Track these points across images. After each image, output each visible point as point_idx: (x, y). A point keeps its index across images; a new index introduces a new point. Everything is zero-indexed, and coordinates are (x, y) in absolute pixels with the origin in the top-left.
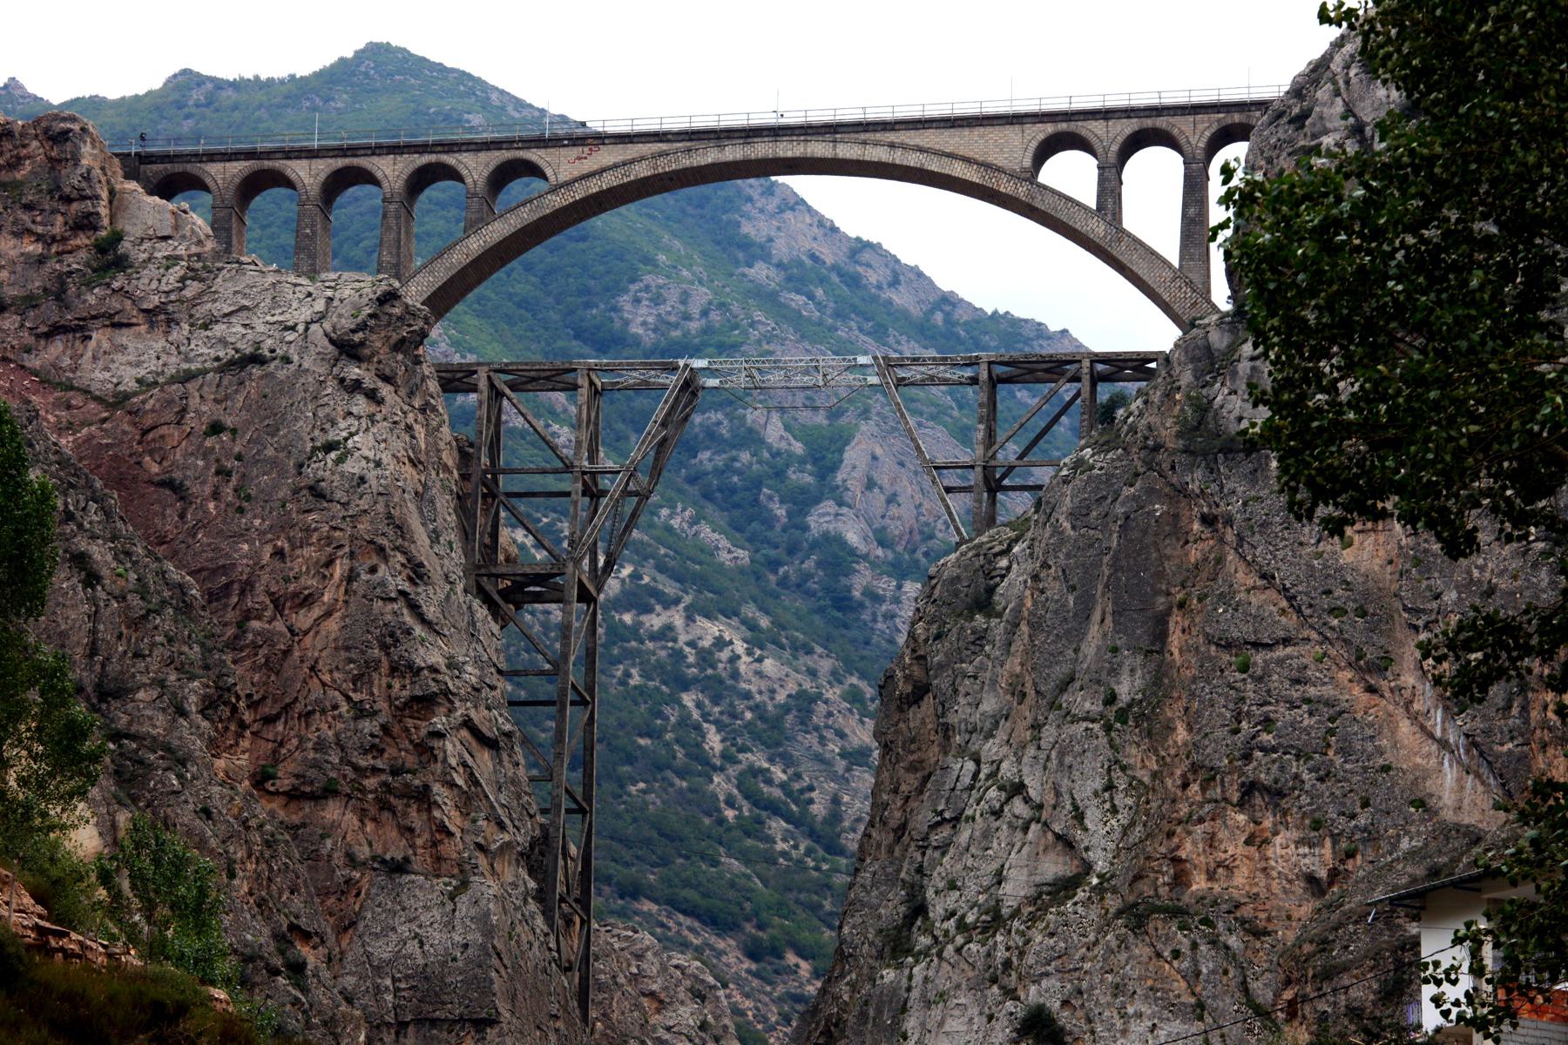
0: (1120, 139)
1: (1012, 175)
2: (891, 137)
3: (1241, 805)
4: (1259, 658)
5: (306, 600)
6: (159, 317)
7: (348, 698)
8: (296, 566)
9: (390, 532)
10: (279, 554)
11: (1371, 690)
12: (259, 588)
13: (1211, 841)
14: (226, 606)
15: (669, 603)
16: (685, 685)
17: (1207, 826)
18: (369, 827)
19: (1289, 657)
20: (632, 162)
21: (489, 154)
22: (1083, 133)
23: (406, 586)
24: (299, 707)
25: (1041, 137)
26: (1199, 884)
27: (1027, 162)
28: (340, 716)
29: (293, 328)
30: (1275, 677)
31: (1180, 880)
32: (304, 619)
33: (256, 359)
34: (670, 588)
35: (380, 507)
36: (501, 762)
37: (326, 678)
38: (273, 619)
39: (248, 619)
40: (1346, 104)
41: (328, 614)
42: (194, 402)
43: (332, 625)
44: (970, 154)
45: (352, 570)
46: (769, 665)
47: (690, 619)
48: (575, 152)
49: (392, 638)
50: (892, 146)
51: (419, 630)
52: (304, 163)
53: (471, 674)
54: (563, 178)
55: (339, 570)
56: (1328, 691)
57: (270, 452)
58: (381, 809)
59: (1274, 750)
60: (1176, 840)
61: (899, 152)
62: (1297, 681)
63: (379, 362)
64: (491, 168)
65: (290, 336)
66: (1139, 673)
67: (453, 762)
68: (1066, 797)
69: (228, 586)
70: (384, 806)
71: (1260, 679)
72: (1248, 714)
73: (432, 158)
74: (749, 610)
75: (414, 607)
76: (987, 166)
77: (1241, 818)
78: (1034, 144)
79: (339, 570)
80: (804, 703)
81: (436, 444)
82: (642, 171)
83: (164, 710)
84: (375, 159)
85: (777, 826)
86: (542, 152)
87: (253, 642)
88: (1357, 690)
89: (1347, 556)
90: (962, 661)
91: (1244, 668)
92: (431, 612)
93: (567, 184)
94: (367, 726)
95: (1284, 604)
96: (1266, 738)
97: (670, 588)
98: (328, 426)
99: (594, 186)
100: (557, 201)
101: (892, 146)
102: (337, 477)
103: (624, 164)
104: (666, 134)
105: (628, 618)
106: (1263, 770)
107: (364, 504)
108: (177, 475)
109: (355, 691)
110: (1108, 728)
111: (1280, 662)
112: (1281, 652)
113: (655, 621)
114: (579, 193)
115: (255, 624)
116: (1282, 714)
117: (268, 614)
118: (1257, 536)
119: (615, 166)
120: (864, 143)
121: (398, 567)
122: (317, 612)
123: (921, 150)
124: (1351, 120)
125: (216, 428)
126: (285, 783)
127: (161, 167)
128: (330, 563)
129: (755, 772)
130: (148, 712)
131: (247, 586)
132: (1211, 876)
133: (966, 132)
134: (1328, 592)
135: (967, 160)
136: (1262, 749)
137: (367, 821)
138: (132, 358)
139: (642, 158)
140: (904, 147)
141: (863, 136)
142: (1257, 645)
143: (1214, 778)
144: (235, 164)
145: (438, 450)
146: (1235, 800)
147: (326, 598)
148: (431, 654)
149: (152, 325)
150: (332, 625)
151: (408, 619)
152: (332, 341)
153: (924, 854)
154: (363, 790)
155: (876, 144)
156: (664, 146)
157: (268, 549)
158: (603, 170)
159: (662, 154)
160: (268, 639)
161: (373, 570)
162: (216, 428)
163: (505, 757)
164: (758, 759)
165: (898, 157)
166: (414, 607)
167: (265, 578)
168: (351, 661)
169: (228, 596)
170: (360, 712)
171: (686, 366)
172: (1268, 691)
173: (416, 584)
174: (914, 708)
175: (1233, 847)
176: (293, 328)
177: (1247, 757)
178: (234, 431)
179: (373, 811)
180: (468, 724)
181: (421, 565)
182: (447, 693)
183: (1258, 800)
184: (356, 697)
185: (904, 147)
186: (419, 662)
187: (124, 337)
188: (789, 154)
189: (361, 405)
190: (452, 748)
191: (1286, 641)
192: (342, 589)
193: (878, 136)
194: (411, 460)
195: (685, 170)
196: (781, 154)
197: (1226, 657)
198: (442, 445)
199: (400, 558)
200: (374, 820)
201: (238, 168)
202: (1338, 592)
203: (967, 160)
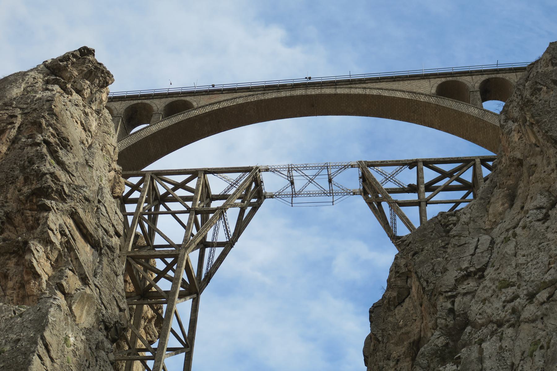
0: (480, 82)
20: (236, 98)
21: (167, 99)
25: (439, 82)
36: (100, 262)
61: (368, 90)
63: (74, 82)
73: (140, 101)
86: (192, 98)
90: (437, 257)
93: (203, 107)
101: (365, 88)
103: (231, 99)
120: (351, 88)
133: (401, 82)
135: (404, 91)
153: (453, 303)
163: (105, 260)
174: (399, 307)
188: (313, 93)
195: (261, 100)
203: (404, 91)
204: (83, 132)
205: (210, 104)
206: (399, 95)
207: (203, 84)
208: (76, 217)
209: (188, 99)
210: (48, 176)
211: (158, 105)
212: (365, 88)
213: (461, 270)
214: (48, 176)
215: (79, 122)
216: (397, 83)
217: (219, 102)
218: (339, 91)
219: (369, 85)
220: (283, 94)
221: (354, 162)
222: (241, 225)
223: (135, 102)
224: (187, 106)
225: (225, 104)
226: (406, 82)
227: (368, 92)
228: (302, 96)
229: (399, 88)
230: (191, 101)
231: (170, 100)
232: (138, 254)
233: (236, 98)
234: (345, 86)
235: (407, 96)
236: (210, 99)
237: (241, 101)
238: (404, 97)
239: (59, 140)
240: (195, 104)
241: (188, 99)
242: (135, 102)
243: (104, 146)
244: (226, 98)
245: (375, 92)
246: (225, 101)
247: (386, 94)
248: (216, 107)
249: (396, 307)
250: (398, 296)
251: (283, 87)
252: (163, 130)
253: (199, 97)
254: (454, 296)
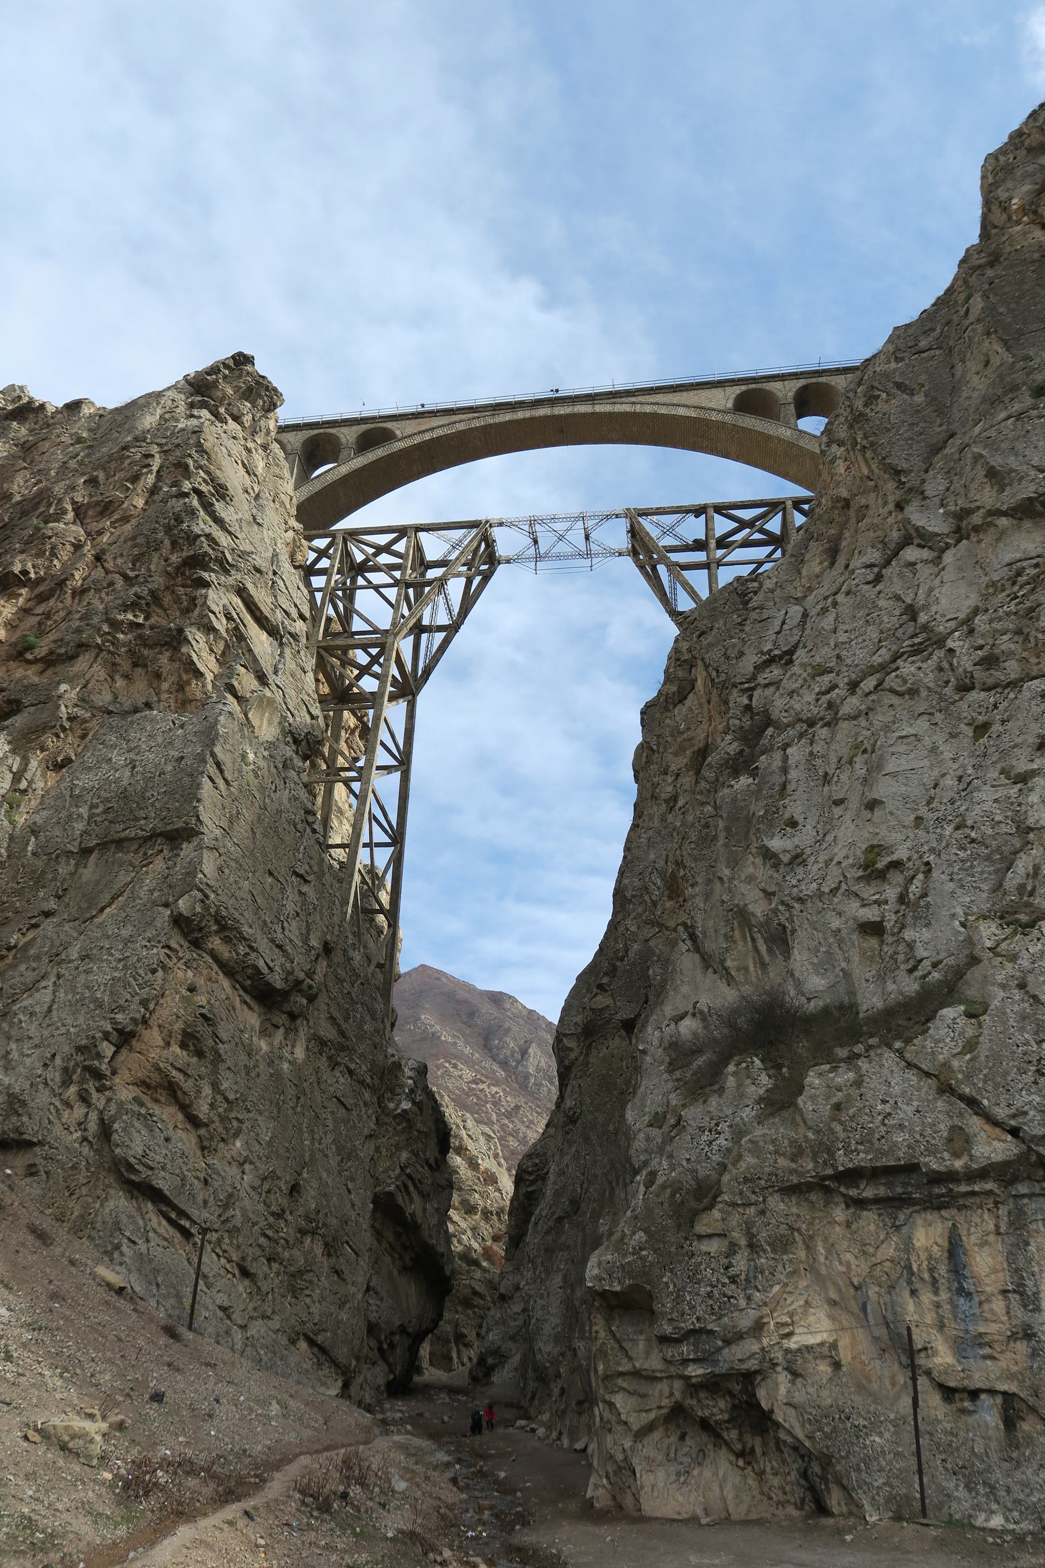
0: (795, 390)
15: (483, 1082)
16: (487, 1102)
18: (120, 683)
25: (738, 392)
34: (484, 1079)
36: (281, 655)
37: (110, 565)
46: (509, 1098)
47: (489, 1086)
58: (135, 665)
61: (639, 406)
63: (229, 404)
70: (138, 662)
73: (322, 431)
74: (504, 1087)
80: (517, 1107)
85: (510, 1138)
86: (394, 423)
90: (732, 638)
93: (410, 436)
97: (484, 1079)
101: (634, 403)
104: (477, 407)
105: (474, 1086)
109: (133, 570)
113: (481, 1086)
129: (504, 1125)
133: (685, 394)
135: (688, 406)
137: (117, 677)
153: (750, 698)
154: (115, 642)
159: (474, 418)
163: (287, 651)
164: (506, 1121)
174: (680, 706)
179: (125, 665)
188: (562, 412)
195: (490, 425)
200: (126, 677)
203: (688, 406)
204: (246, 476)
205: (420, 432)
206: (681, 411)
207: (408, 404)
208: (245, 595)
209: (389, 425)
210: (202, 539)
211: (348, 436)
212: (634, 403)
213: (762, 653)
214: (202, 539)
215: (239, 462)
216: (678, 394)
217: (432, 429)
218: (599, 408)
219: (640, 399)
220: (520, 415)
221: (619, 509)
222: (469, 601)
223: (316, 432)
224: (387, 436)
225: (440, 432)
226: (691, 393)
227: (638, 408)
228: (546, 417)
230: (393, 428)
231: (364, 427)
232: (331, 643)
234: (606, 401)
235: (692, 413)
236: (419, 424)
237: (461, 427)
238: (688, 414)
239: (214, 487)
240: (398, 433)
241: (389, 425)
242: (316, 432)
243: (277, 495)
244: (441, 423)
245: (648, 409)
246: (440, 428)
247: (663, 410)
248: (427, 436)
249: (675, 706)
250: (679, 692)
251: (520, 405)
252: (356, 471)
253: (404, 422)
254: (753, 689)
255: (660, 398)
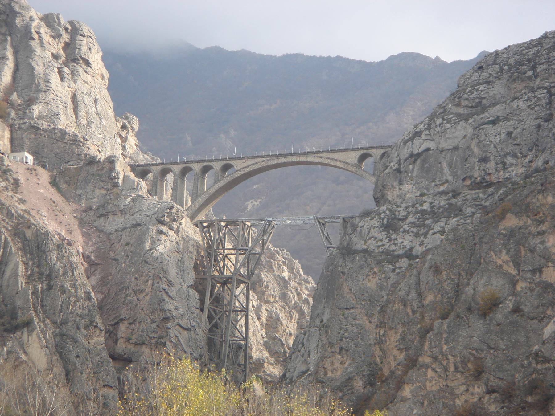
0: (380, 154)
1: (352, 165)
2: (321, 155)
3: (340, 353)
4: (347, 312)
5: (142, 291)
6: (123, 212)
7: (150, 318)
8: (140, 282)
9: (162, 273)
10: (136, 279)
11: (370, 322)
12: (130, 288)
13: (332, 363)
14: (122, 293)
17: (331, 359)
19: (353, 312)
20: (256, 163)
22: (371, 153)
23: (166, 287)
24: (138, 320)
25: (360, 154)
26: (330, 374)
27: (356, 161)
28: (148, 322)
29: (149, 216)
30: (350, 318)
31: (326, 374)
32: (141, 296)
33: (138, 225)
35: (161, 266)
37: (145, 312)
38: (134, 296)
39: (127, 296)
40: (398, 153)
41: (147, 295)
42: (124, 237)
43: (148, 298)
44: (341, 160)
45: (153, 283)
48: (242, 161)
49: (161, 301)
50: (321, 157)
51: (167, 299)
52: (176, 166)
53: (181, 311)
54: (239, 168)
55: (150, 283)
56: (360, 322)
57: (138, 251)
59: (347, 338)
60: (324, 362)
62: (354, 319)
64: (221, 166)
65: (148, 218)
66: (329, 314)
67: (172, 335)
68: (308, 348)
69: (123, 288)
71: (346, 318)
72: (343, 328)
75: (167, 293)
76: (345, 163)
77: (339, 357)
78: (358, 156)
79: (150, 283)
81: (187, 246)
82: (258, 166)
83: (73, 328)
84: (193, 164)
86: (234, 161)
87: (128, 303)
88: (367, 322)
89: (369, 285)
91: (343, 315)
92: (171, 294)
94: (154, 326)
95: (354, 297)
96: (346, 334)
98: (153, 243)
99: (246, 171)
100: (237, 175)
101: (321, 157)
102: (151, 258)
103: (254, 164)
106: (344, 344)
107: (157, 265)
108: (117, 257)
109: (152, 316)
110: (320, 330)
111: (351, 314)
112: (352, 311)
114: (242, 172)
115: (129, 298)
116: (350, 328)
117: (132, 295)
118: (350, 279)
119: (252, 165)
120: (314, 157)
121: (164, 282)
122: (144, 294)
123: (329, 158)
124: (398, 158)
125: (128, 244)
126: (133, 341)
127: (141, 168)
128: (147, 281)
130: (70, 329)
131: (128, 288)
132: (332, 372)
134: (363, 295)
135: (340, 161)
136: (345, 338)
138: (116, 223)
139: (259, 162)
140: (325, 158)
141: (314, 155)
142: (346, 309)
143: (333, 346)
144: (159, 166)
145: (188, 248)
146: (338, 352)
147: (146, 291)
148: (170, 306)
149: (122, 214)
150: (148, 298)
151: (165, 296)
152: (156, 220)
154: (151, 343)
155: (318, 157)
156: (264, 159)
157: (134, 278)
158: (249, 166)
160: (131, 302)
161: (158, 283)
162: (128, 244)
165: (322, 161)
166: (167, 293)
167: (132, 285)
168: (151, 308)
169: (123, 290)
170: (153, 322)
171: (266, 220)
172: (348, 322)
173: (169, 286)
175: (337, 365)
176: (149, 216)
177: (341, 340)
178: (132, 245)
180: (179, 325)
181: (170, 281)
182: (172, 317)
183: (344, 352)
184: (152, 317)
185: (325, 158)
186: (166, 308)
187: (116, 218)
188: (296, 161)
189: (163, 237)
190: (172, 332)
191: (353, 308)
192: (150, 288)
193: (318, 155)
194: (176, 251)
196: (293, 160)
197: (340, 312)
198: (189, 246)
199: (165, 280)
201: (160, 167)
202: (366, 294)
203: (340, 161)
205: (243, 168)
215: (175, 252)
217: (248, 167)
229: (339, 159)
230: (234, 164)
233: (256, 163)
255: (331, 155)
